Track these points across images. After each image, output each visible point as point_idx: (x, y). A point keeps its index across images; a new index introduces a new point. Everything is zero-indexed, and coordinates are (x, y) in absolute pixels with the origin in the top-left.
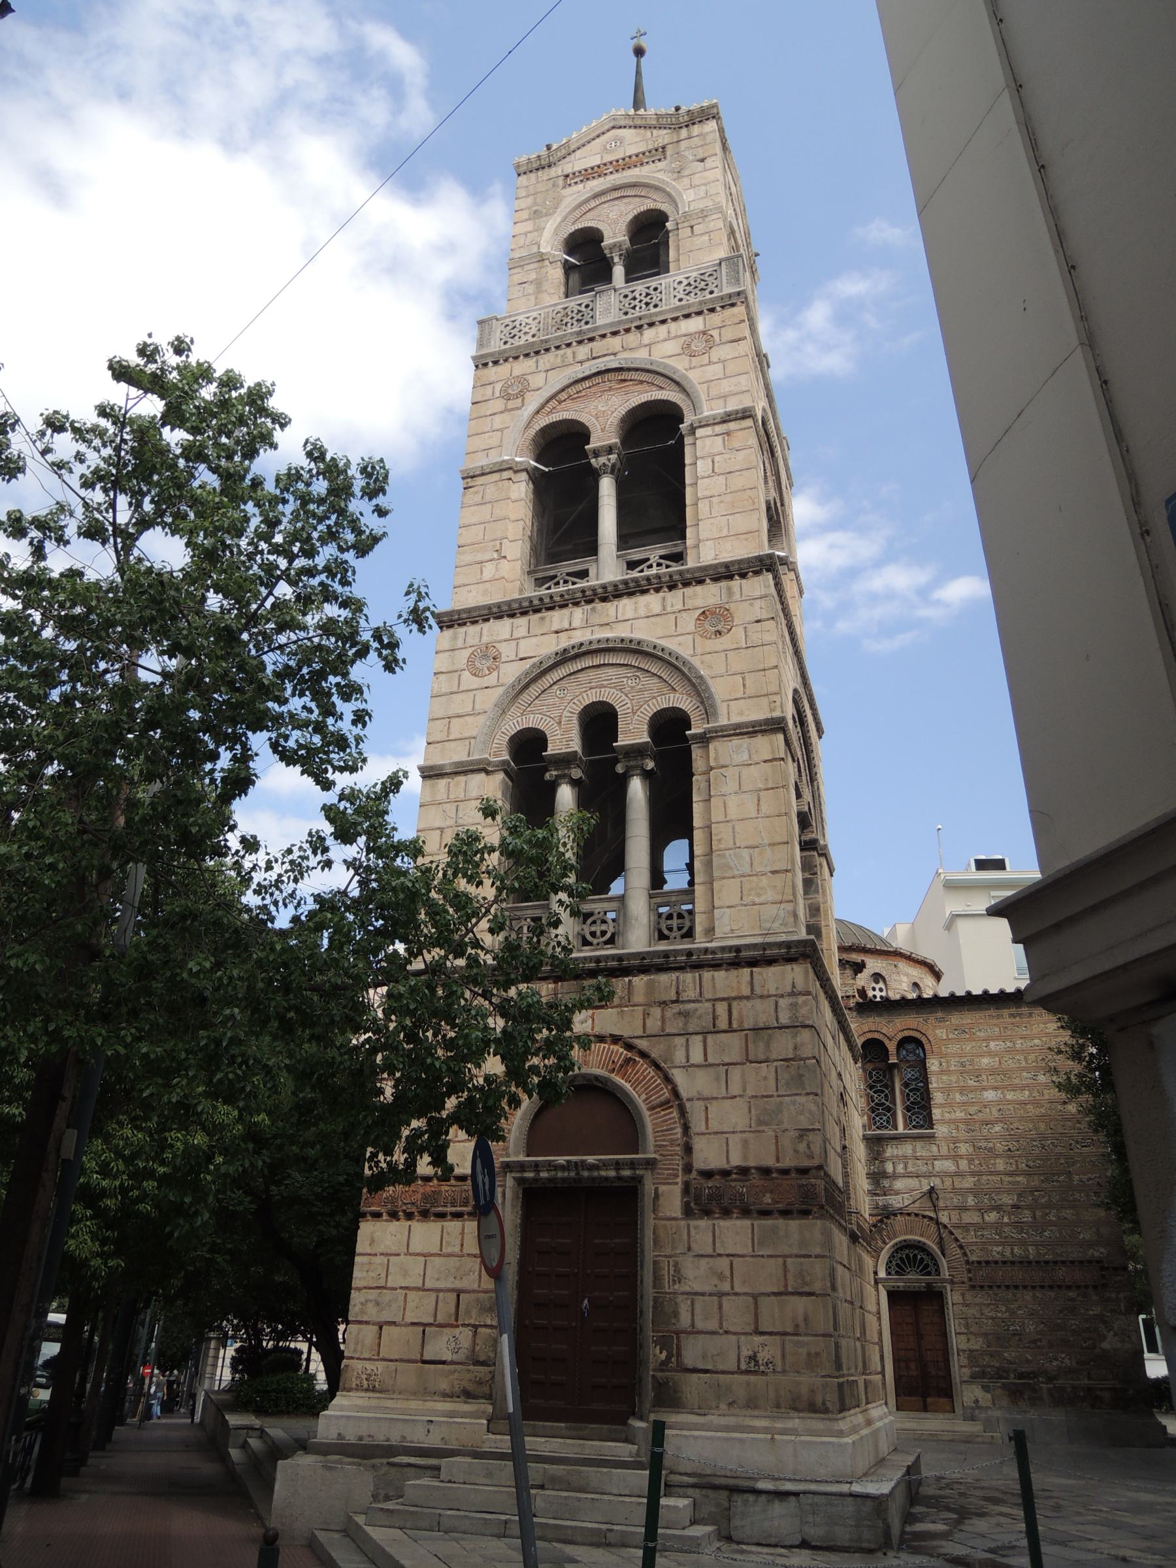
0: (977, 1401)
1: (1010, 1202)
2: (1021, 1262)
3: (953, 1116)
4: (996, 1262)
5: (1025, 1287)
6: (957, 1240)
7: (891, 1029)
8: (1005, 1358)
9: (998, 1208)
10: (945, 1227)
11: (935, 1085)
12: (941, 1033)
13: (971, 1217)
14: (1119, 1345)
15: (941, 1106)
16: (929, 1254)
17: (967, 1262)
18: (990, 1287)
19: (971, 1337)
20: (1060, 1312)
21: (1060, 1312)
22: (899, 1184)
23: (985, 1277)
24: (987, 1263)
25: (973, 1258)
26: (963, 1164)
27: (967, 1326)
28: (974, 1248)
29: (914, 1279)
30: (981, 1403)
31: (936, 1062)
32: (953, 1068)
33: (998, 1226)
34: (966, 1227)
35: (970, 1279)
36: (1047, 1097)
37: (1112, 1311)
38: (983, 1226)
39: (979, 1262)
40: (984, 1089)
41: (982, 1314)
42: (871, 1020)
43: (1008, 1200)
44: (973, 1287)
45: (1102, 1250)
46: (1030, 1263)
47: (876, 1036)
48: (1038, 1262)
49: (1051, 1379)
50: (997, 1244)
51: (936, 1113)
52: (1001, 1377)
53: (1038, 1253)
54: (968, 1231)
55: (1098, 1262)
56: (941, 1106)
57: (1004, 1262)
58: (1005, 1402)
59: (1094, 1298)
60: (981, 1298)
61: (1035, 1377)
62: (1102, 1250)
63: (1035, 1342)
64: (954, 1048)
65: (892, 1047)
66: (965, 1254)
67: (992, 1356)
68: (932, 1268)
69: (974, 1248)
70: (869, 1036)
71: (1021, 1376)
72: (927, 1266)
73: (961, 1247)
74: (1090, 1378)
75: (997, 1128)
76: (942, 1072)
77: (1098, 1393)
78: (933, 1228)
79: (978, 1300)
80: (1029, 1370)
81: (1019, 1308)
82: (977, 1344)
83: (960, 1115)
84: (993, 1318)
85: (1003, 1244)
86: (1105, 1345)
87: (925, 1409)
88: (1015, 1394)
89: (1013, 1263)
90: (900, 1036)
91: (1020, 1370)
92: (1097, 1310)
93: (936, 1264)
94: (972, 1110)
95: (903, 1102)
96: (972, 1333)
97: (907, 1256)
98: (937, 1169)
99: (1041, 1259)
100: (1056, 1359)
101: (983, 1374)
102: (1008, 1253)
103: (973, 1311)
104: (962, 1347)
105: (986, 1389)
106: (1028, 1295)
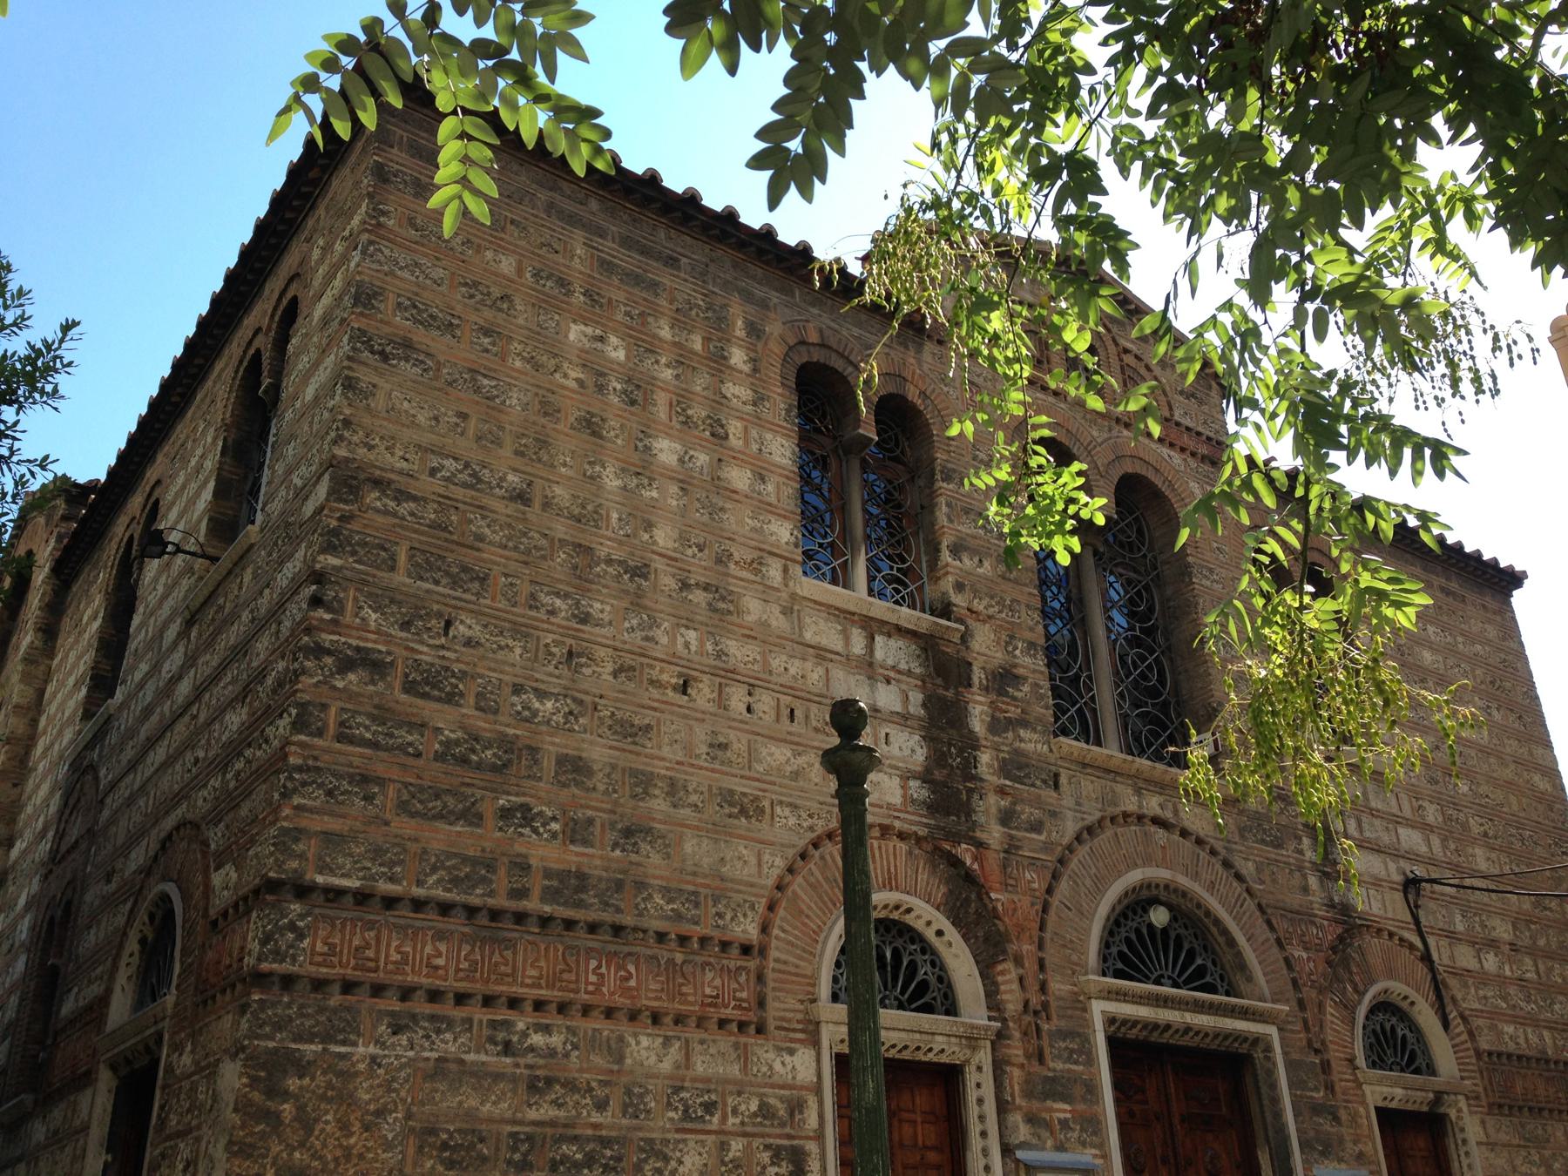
4: (1509, 1056)
9: (1493, 944)
13: (1465, 958)
24: (1499, 1055)
36: (1508, 750)
38: (1483, 979)
39: (1490, 1054)
46: (1547, 1061)
57: (1520, 1057)
69: (1480, 1022)
78: (1421, 970)
79: (1503, 1137)
98: (1405, 845)
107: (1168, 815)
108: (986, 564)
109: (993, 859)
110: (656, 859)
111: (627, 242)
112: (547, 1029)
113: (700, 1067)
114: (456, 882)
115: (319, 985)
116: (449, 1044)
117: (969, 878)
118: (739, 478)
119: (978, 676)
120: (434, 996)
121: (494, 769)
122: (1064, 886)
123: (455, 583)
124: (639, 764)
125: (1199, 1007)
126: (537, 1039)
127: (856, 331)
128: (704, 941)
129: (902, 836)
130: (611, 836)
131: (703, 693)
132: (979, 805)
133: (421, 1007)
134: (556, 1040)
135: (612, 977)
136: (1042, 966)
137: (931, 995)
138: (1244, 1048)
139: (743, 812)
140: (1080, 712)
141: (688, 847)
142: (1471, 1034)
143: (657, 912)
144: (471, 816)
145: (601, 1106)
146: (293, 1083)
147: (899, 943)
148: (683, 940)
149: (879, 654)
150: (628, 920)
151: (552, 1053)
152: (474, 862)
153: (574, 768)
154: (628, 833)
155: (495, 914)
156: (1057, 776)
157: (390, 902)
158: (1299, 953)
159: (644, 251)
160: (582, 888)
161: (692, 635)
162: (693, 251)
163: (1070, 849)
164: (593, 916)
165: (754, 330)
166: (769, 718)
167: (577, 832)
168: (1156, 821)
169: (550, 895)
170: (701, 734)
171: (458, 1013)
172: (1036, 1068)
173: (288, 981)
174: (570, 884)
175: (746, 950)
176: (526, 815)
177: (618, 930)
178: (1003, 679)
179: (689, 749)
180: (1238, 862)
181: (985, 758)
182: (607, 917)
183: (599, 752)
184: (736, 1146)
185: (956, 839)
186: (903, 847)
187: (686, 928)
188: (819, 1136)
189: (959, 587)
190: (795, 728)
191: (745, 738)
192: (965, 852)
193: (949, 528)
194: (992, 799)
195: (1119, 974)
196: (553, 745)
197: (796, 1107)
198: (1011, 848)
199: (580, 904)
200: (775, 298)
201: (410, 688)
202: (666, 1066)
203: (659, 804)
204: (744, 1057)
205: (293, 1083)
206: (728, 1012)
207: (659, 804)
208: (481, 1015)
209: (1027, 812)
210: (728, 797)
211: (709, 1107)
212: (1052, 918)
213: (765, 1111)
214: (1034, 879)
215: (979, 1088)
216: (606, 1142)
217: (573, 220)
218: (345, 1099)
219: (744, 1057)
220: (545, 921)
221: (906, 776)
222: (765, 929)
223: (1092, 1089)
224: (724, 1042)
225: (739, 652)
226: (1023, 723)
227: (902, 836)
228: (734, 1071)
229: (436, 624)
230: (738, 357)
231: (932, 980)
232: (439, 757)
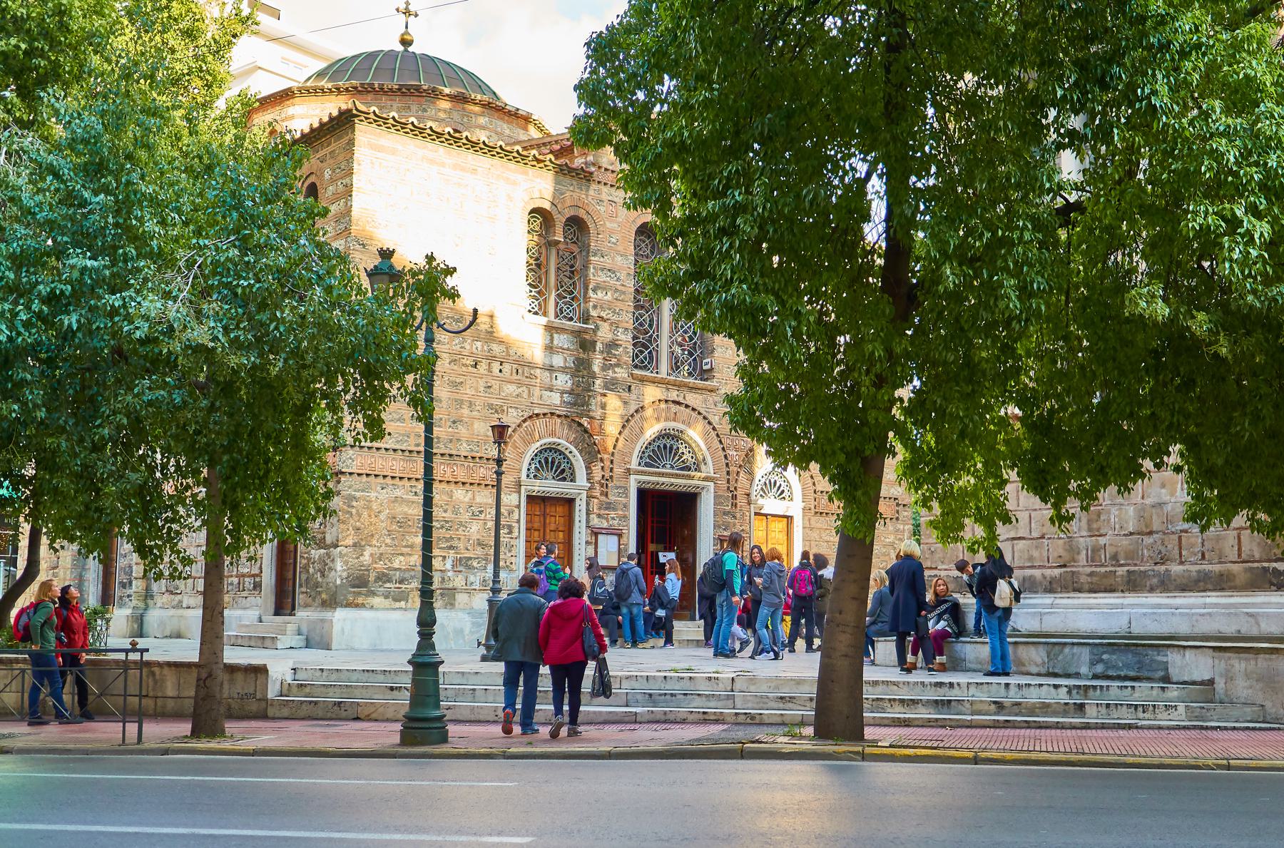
79: (819, 525)
111: (455, 167)
113: (478, 500)
115: (359, 475)
116: (398, 493)
117: (586, 431)
119: (599, 346)
120: (393, 478)
125: (677, 476)
129: (559, 416)
131: (483, 367)
132: (593, 401)
133: (389, 480)
135: (449, 471)
136: (612, 462)
137: (565, 473)
140: (650, 353)
141: (476, 426)
143: (464, 449)
145: (445, 511)
146: (354, 503)
149: (555, 342)
150: (454, 452)
154: (454, 422)
155: (410, 452)
158: (731, 453)
159: (463, 169)
161: (479, 344)
163: (632, 416)
166: (508, 375)
168: (674, 402)
170: (482, 383)
171: (400, 483)
172: (603, 498)
173: (351, 474)
177: (451, 455)
178: (612, 345)
180: (710, 417)
181: (598, 382)
182: (447, 452)
186: (559, 421)
187: (474, 454)
188: (518, 521)
189: (595, 307)
192: (584, 421)
193: (595, 277)
194: (599, 398)
195: (647, 465)
200: (520, 178)
202: (467, 499)
203: (465, 411)
205: (354, 503)
207: (465, 411)
208: (407, 484)
210: (491, 406)
211: (481, 512)
215: (580, 506)
216: (447, 522)
217: (432, 162)
218: (369, 508)
221: (562, 393)
223: (626, 506)
226: (618, 365)
227: (559, 416)
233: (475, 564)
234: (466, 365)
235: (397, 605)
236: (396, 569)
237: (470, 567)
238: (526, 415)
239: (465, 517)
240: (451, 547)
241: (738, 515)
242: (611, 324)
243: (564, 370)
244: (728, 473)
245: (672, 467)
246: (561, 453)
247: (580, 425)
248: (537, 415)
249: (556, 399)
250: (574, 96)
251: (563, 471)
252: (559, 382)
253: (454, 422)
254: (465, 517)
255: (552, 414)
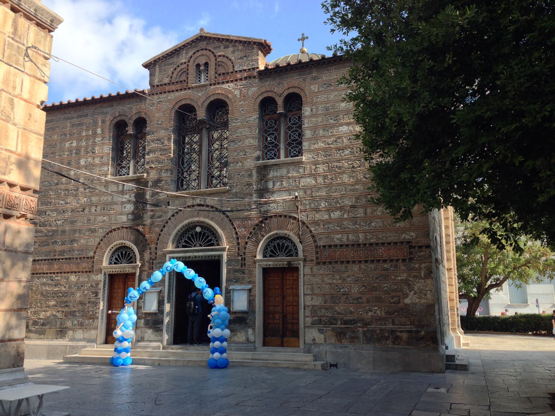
0: (314, 340)
1: (350, 203)
2: (353, 245)
3: (316, 146)
4: (336, 246)
5: (354, 262)
6: (311, 231)
7: (279, 89)
8: (336, 311)
9: (341, 209)
10: (304, 223)
11: (306, 125)
12: (314, 88)
14: (417, 300)
15: (309, 139)
16: (292, 242)
17: (316, 247)
18: (330, 263)
19: (314, 297)
20: (377, 278)
21: (377, 278)
22: (277, 197)
23: (328, 255)
24: (330, 246)
25: (321, 243)
26: (320, 180)
27: (312, 290)
28: (322, 236)
29: (281, 261)
30: (317, 341)
31: (308, 109)
32: (320, 112)
33: (340, 221)
34: (316, 223)
35: (317, 258)
37: (414, 276)
39: (324, 246)
40: (341, 125)
41: (323, 281)
42: (267, 83)
43: (348, 202)
44: (318, 263)
45: (412, 234)
46: (359, 245)
47: (270, 94)
48: (365, 245)
49: (366, 324)
50: (338, 233)
51: (305, 145)
52: (332, 324)
53: (366, 239)
54: (319, 225)
55: (409, 242)
56: (309, 139)
58: (333, 340)
59: (402, 268)
60: (323, 270)
61: (355, 323)
62: (412, 234)
63: (358, 298)
64: (322, 98)
65: (280, 101)
66: (315, 241)
67: (327, 309)
68: (294, 252)
69: (322, 236)
70: (265, 95)
71: (346, 322)
72: (291, 250)
73: (313, 236)
74: (393, 323)
75: (347, 152)
76: (312, 116)
77: (398, 334)
79: (321, 272)
80: (351, 318)
81: (349, 276)
82: (318, 301)
83: (321, 145)
84: (330, 284)
85: (342, 233)
86: (407, 301)
87: (282, 345)
88: (340, 335)
89: (347, 245)
90: (286, 93)
91: (345, 319)
92: (404, 276)
93: (296, 249)
94: (330, 141)
95: (286, 140)
96: (315, 294)
97: (278, 244)
99: (368, 242)
100: (371, 311)
101: (320, 322)
102: (345, 239)
103: (318, 279)
104: (307, 303)
105: (321, 331)
106: (356, 268)
107: (202, 203)
108: (156, 153)
109: (147, 229)
110: (76, 245)
112: (57, 277)
113: (81, 280)
114: (46, 256)
118: (97, 161)
121: (52, 236)
122: (165, 229)
123: (47, 205)
124: (74, 228)
126: (56, 278)
127: (128, 106)
128: (84, 258)
129: (126, 228)
130: (69, 242)
132: (145, 215)
134: (59, 278)
135: (68, 266)
136: (156, 248)
137: (131, 259)
138: (217, 258)
139: (92, 232)
142: (315, 241)
143: (76, 254)
144: (48, 245)
147: (126, 250)
148: (81, 258)
150: (71, 257)
151: (58, 280)
152: (48, 252)
153: (64, 232)
154: (72, 241)
156: (169, 202)
157: (38, 260)
160: (64, 253)
162: (89, 110)
163: (170, 219)
164: (65, 257)
165: (103, 122)
167: (63, 243)
169: (59, 255)
170: (85, 219)
174: (62, 252)
175: (91, 258)
176: (56, 242)
179: (83, 223)
183: (67, 228)
184: (86, 292)
185: (138, 225)
186: (125, 230)
190: (105, 211)
191: (93, 217)
192: (140, 228)
196: (60, 229)
197: (97, 284)
198: (152, 224)
199: (64, 255)
201: (40, 226)
204: (89, 277)
206: (87, 270)
209: (158, 214)
211: (82, 286)
212: (161, 237)
213: (92, 286)
214: (158, 230)
216: (65, 293)
219: (89, 277)
220: (59, 259)
222: (95, 252)
224: (85, 275)
225: (94, 199)
228: (87, 279)
229: (44, 213)
230: (99, 131)
231: (133, 256)
232: (44, 236)
233: (77, 314)
234: (78, 212)
235: (40, 337)
236: (41, 319)
237: (74, 316)
238: (107, 231)
239: (74, 289)
240: (66, 306)
241: (246, 271)
242: (157, 170)
243: (129, 202)
244: (238, 244)
245: (201, 245)
246: (130, 248)
247: (138, 231)
248: (115, 230)
249: (124, 218)
250: (272, 47)
251: (131, 257)
252: (126, 209)
253: (72, 241)
254: (74, 289)
255: (123, 227)
